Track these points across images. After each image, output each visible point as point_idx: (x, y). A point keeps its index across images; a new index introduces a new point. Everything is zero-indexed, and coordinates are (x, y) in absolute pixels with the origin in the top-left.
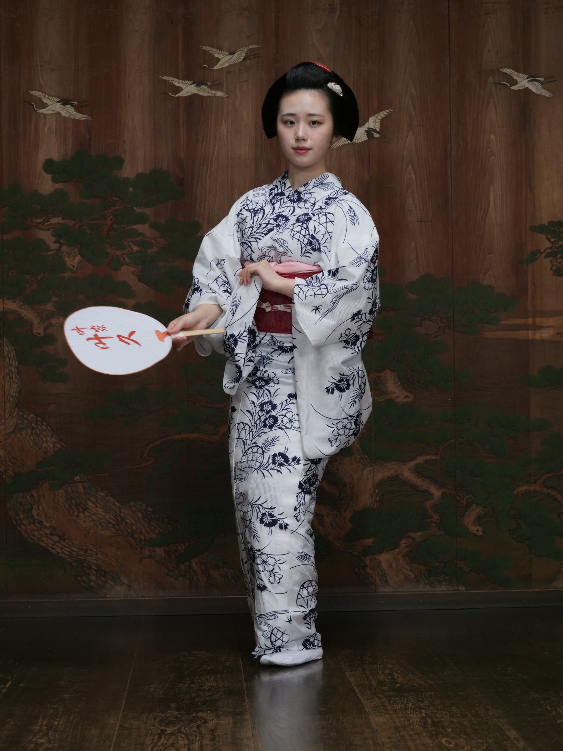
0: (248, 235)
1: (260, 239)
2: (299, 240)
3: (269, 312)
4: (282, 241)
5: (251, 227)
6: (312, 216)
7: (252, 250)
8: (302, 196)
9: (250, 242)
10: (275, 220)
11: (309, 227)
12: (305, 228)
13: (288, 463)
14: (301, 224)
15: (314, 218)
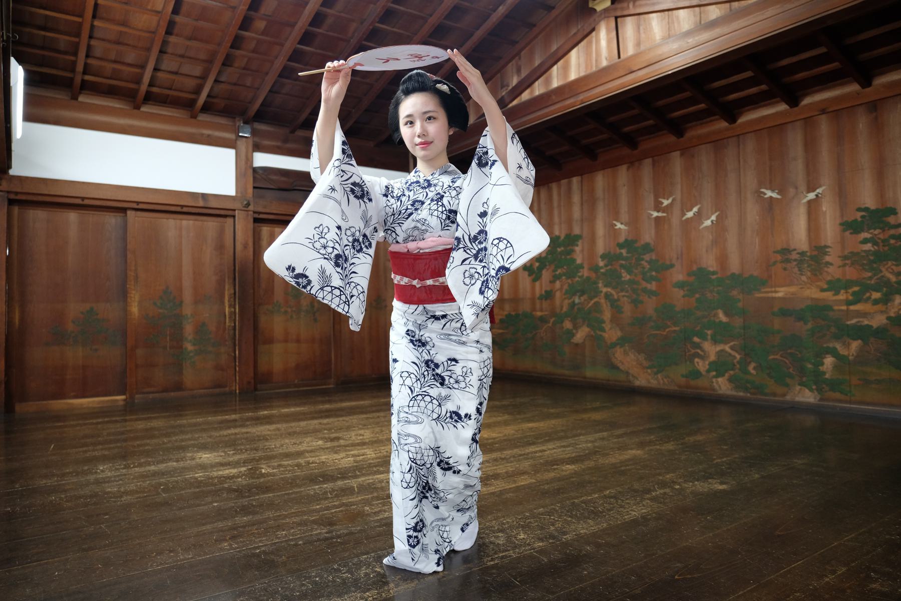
0: (391, 221)
1: (403, 224)
2: (438, 217)
3: (420, 287)
4: (423, 220)
5: (392, 215)
6: (444, 194)
7: (396, 234)
8: (431, 183)
9: (393, 228)
10: (412, 205)
11: (444, 204)
12: (441, 206)
13: (461, 420)
14: (436, 202)
15: (445, 195)
